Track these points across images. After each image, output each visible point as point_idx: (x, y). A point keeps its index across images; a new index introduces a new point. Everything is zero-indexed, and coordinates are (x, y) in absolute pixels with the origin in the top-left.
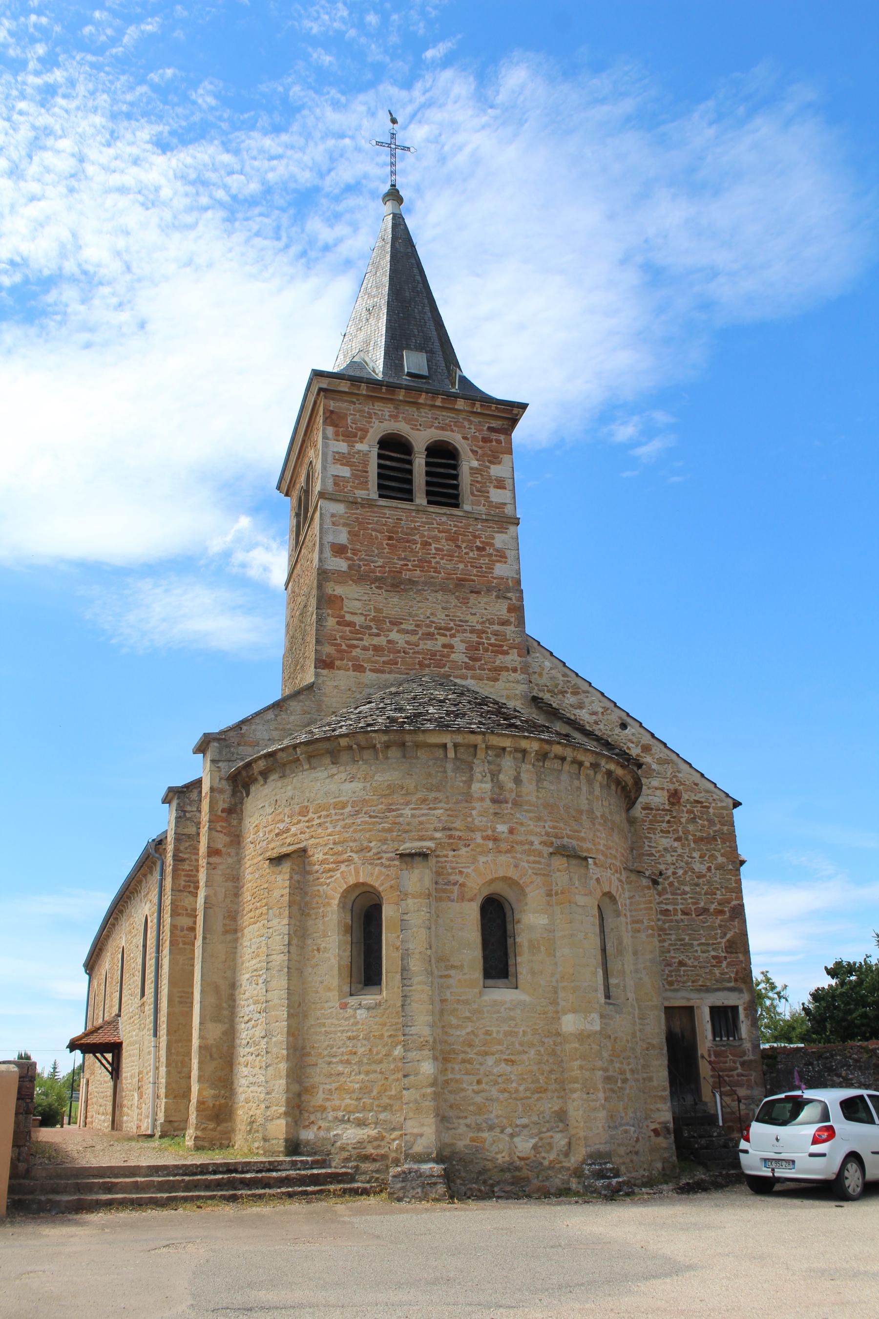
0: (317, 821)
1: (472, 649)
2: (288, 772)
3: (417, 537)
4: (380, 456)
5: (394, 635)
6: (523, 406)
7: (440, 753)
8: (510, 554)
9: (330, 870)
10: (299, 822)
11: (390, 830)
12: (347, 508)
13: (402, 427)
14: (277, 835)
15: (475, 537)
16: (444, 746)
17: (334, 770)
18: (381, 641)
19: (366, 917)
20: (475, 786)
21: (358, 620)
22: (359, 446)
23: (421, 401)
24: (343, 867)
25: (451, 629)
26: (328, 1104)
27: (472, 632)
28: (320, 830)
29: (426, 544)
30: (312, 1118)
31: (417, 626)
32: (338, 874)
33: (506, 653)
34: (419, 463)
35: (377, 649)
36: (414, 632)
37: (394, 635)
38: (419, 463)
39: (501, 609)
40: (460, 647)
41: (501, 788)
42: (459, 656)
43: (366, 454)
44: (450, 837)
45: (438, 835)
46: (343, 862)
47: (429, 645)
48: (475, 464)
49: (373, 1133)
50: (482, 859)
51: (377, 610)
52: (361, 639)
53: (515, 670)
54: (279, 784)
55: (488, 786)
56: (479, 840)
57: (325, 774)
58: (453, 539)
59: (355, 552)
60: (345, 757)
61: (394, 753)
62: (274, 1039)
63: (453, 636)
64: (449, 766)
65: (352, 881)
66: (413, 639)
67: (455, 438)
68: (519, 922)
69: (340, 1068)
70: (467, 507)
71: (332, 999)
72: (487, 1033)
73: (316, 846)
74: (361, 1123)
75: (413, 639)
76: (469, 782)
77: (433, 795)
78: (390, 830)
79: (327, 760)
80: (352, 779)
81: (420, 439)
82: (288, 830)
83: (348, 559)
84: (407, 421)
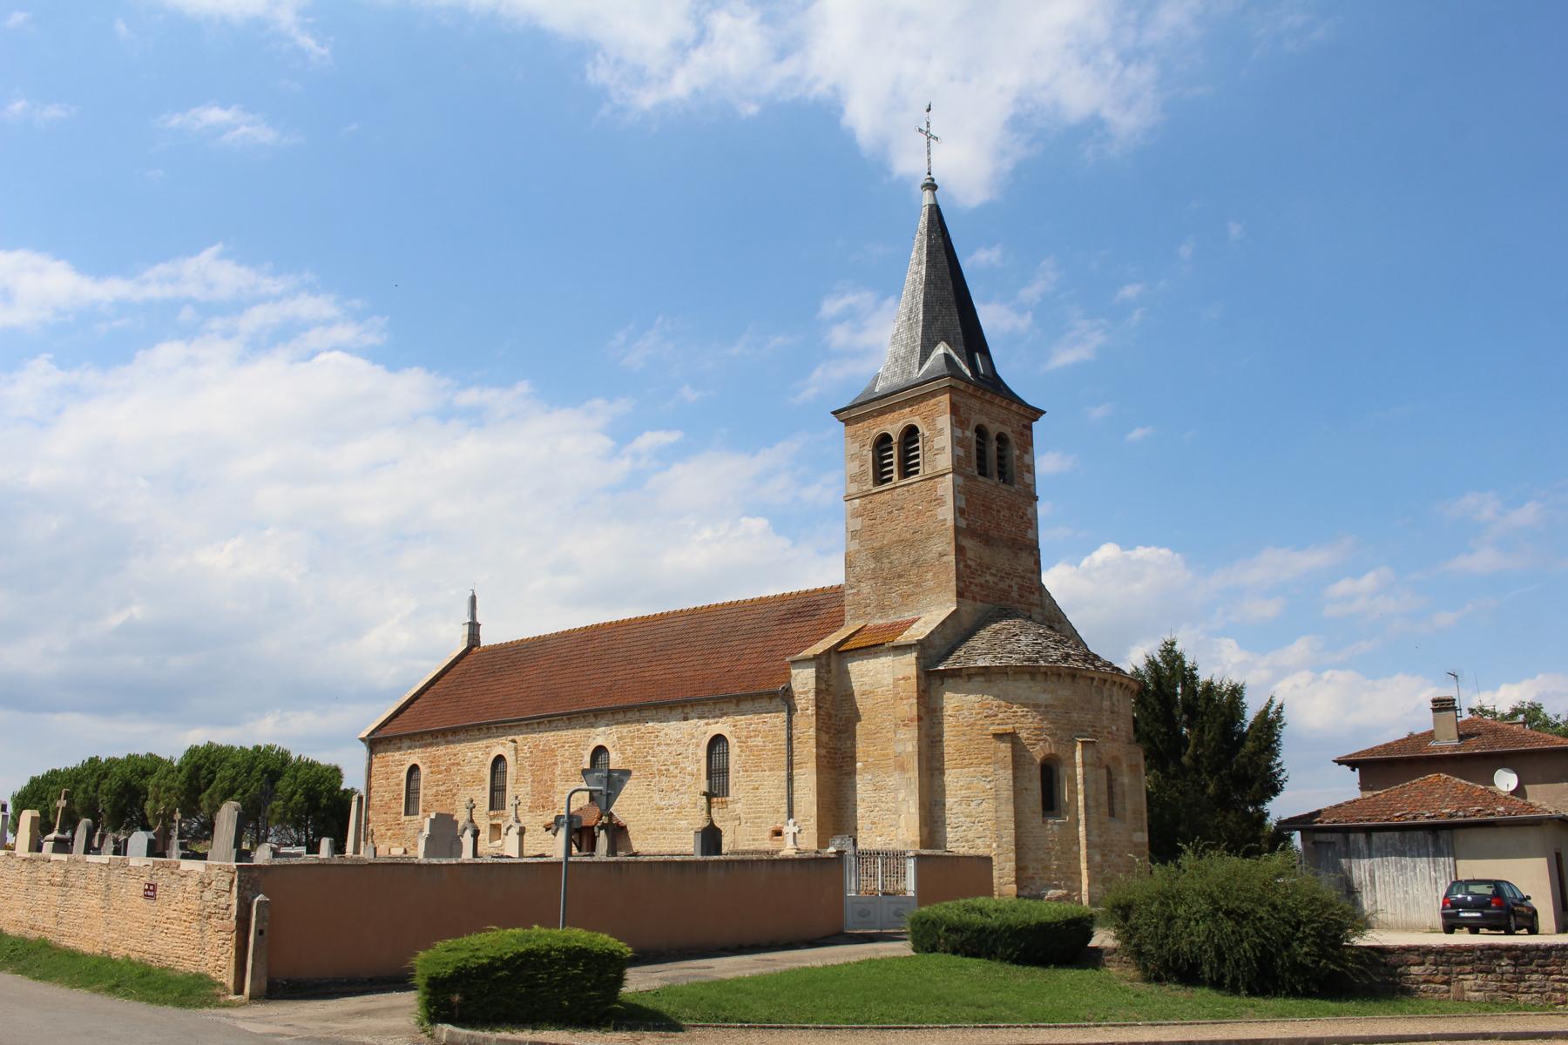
1: (1021, 588)
13: (984, 420)
18: (982, 580)
19: (1050, 774)
21: (972, 564)
34: (993, 447)
38: (993, 447)
39: (1030, 563)
40: (1015, 588)
42: (1015, 594)
47: (1002, 585)
60: (1039, 677)
61: (1068, 680)
67: (1007, 430)
71: (1039, 819)
74: (1057, 887)
79: (1027, 677)
81: (994, 429)
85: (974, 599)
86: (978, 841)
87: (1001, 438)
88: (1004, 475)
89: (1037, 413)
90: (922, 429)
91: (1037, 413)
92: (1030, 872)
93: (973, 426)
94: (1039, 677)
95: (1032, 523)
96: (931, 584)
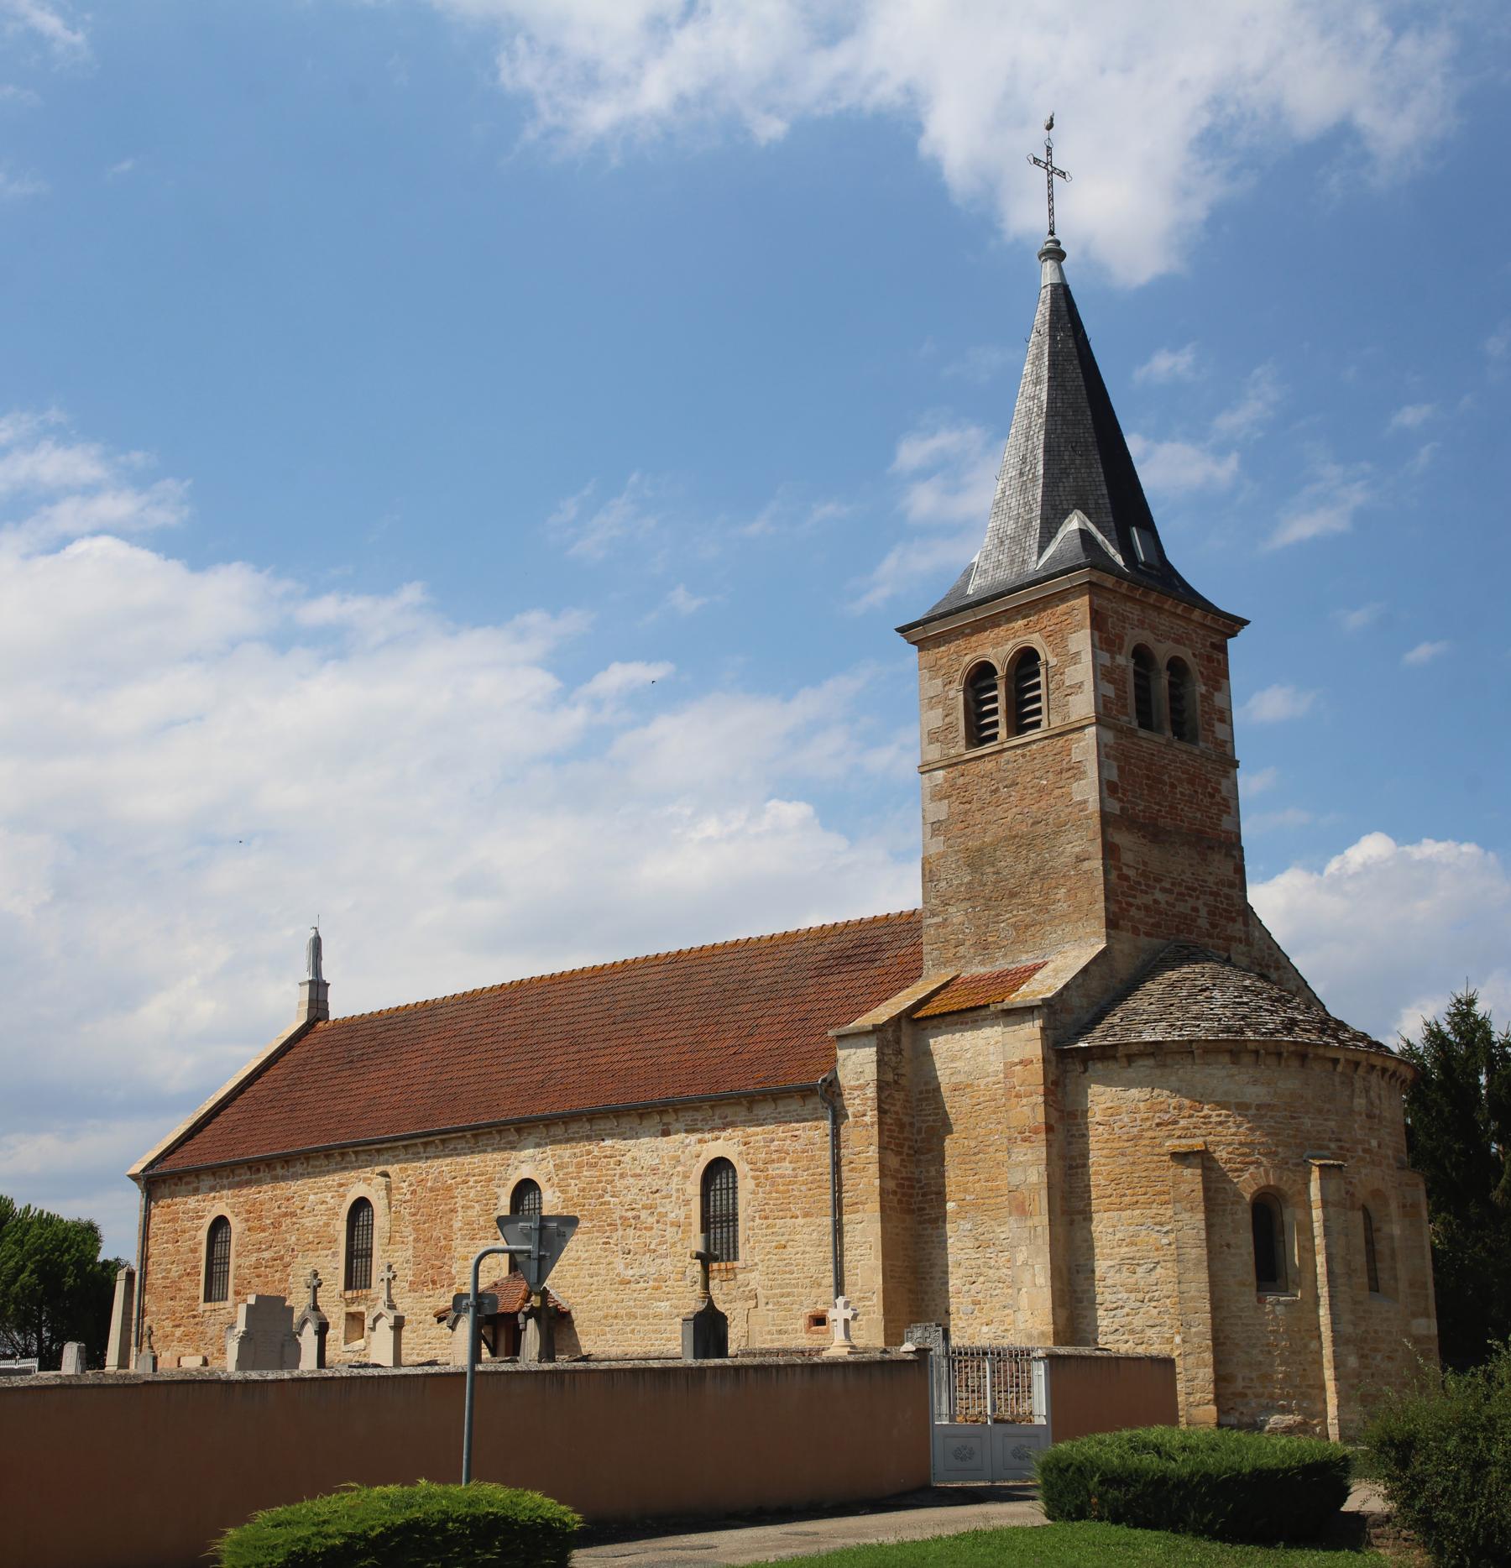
0: (1214, 1119)
2: (1169, 1061)
3: (1166, 778)
4: (1135, 672)
5: (1158, 895)
6: (1247, 622)
7: (1329, 1065)
8: (1232, 804)
9: (1236, 1170)
10: (1191, 1116)
11: (1295, 1136)
12: (1116, 737)
13: (1145, 636)
14: (1158, 1125)
15: (1208, 781)
16: (1335, 1061)
17: (1234, 1070)
18: (1147, 899)
19: (1268, 1219)
20: (1357, 1101)
21: (1131, 873)
22: (1121, 660)
23: (1166, 607)
24: (1252, 1169)
25: (1194, 890)
26: (1249, 1392)
27: (1211, 894)
28: (1220, 1129)
29: (1173, 786)
30: (1231, 1405)
31: (1173, 884)
32: (1247, 1175)
33: (1234, 920)
35: (1147, 908)
36: (1170, 891)
37: (1158, 895)
39: (1227, 870)
40: (1203, 912)
41: (1372, 1103)
42: (1203, 922)
43: (1124, 670)
44: (1341, 1148)
45: (1333, 1145)
46: (1252, 1163)
47: (1181, 908)
48: (1203, 689)
49: (1299, 1418)
50: (1364, 1171)
51: (1145, 864)
52: (1135, 897)
53: (1241, 941)
54: (1158, 1072)
55: (1363, 1101)
56: (1360, 1153)
57: (1224, 1073)
58: (1191, 782)
59: (1125, 791)
60: (1247, 1059)
61: (1294, 1063)
62: (1193, 1330)
63: (1198, 898)
64: (1337, 1079)
65: (1263, 1182)
66: (1171, 898)
67: (1185, 653)
68: (1378, 1230)
69: (1261, 1358)
70: (1202, 744)
71: (1249, 1296)
72: (1376, 1332)
73: (1218, 1144)
74: (1284, 1410)
75: (1171, 898)
76: (1351, 1097)
77: (1327, 1106)
78: (1295, 1136)
79: (1226, 1059)
80: (1255, 1082)
81: (1163, 651)
82: (1176, 1122)
83: (1121, 800)
84: (1153, 628)
85: (1136, 931)
86: (1150, 1332)
87: (1177, 666)
88: (1183, 728)
89: (1235, 624)
90: (1046, 653)
91: (1235, 624)
92: (1239, 1384)
93: (1129, 647)
94: (1247, 1059)
95: (1229, 805)
96: (1062, 906)
